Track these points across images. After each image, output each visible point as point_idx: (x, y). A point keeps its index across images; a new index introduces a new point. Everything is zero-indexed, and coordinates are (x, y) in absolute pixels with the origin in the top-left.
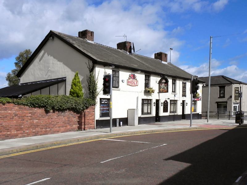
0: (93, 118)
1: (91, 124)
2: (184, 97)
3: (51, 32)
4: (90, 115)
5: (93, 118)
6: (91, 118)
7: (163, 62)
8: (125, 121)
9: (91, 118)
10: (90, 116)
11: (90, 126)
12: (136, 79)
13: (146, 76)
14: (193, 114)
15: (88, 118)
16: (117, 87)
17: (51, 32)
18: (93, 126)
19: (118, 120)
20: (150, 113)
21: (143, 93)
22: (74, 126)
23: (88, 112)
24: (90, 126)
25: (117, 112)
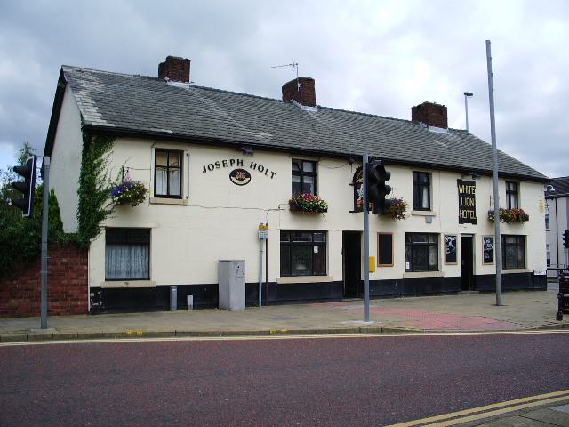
0: (84, 282)
1: (77, 300)
2: (465, 225)
3: (187, 62)
4: (74, 272)
5: (84, 282)
6: (75, 282)
7: (433, 129)
8: (207, 296)
9: (75, 282)
10: (74, 275)
11: (74, 303)
12: (25, 170)
13: (294, 163)
14: (502, 275)
15: (65, 282)
16: (180, 197)
17: (187, 62)
18: (82, 306)
19: (174, 290)
20: (322, 270)
21: (287, 212)
22: (13, 301)
23: (62, 264)
24: (74, 303)
25: (174, 263)
